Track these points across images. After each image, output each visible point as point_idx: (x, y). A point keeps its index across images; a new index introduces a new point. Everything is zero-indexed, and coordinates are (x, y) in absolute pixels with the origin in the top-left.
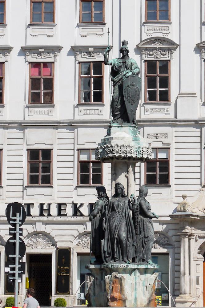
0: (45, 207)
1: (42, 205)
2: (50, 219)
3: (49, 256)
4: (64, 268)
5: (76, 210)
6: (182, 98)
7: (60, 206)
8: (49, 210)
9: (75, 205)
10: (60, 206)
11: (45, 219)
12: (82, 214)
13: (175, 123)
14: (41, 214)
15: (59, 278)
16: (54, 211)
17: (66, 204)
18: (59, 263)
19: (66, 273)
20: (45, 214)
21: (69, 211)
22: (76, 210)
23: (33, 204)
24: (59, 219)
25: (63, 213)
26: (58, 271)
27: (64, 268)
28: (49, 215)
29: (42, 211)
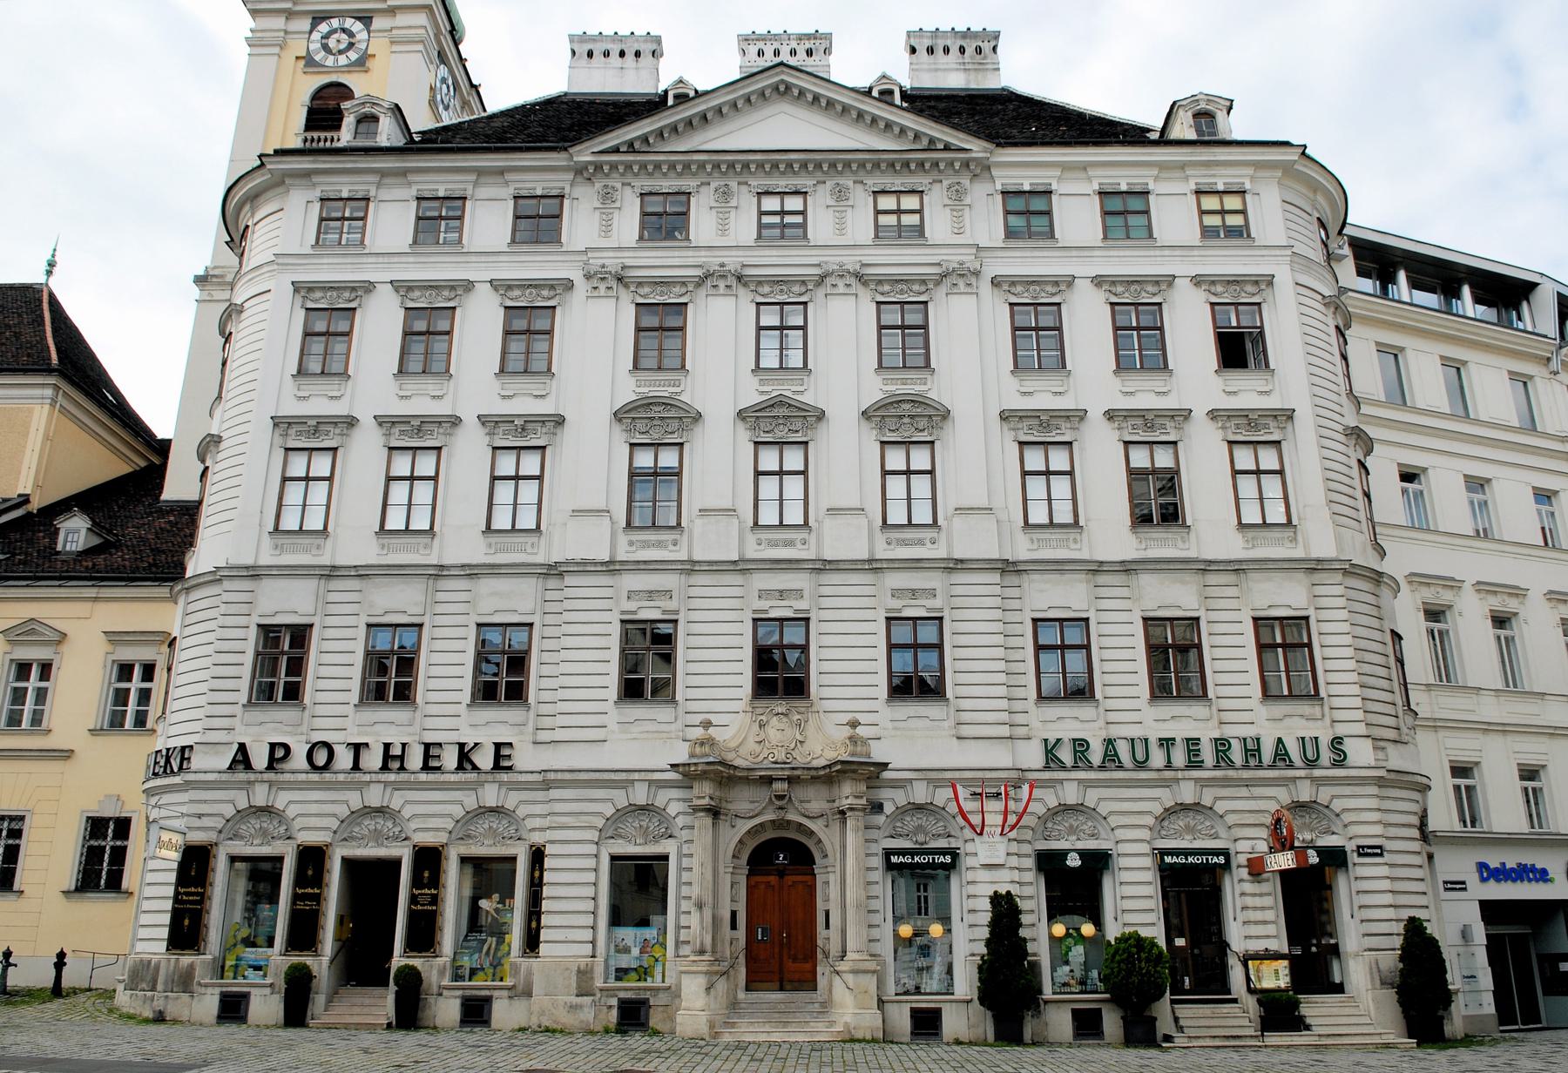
0: (396, 751)
1: (387, 746)
2: (403, 776)
3: (395, 864)
4: (427, 891)
5: (465, 757)
6: (706, 520)
7: (427, 746)
8: (401, 758)
9: (462, 746)
10: (427, 746)
11: (392, 777)
12: (475, 768)
13: (691, 567)
14: (385, 768)
15: (412, 916)
16: (415, 760)
17: (440, 744)
18: (416, 881)
19: (431, 904)
20: (395, 765)
21: (450, 759)
22: (465, 757)
23: (367, 744)
24: (423, 777)
25: (433, 763)
26: (413, 899)
27: (427, 891)
28: (402, 768)
29: (387, 756)
